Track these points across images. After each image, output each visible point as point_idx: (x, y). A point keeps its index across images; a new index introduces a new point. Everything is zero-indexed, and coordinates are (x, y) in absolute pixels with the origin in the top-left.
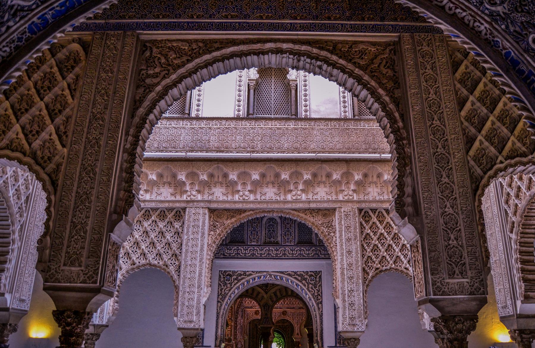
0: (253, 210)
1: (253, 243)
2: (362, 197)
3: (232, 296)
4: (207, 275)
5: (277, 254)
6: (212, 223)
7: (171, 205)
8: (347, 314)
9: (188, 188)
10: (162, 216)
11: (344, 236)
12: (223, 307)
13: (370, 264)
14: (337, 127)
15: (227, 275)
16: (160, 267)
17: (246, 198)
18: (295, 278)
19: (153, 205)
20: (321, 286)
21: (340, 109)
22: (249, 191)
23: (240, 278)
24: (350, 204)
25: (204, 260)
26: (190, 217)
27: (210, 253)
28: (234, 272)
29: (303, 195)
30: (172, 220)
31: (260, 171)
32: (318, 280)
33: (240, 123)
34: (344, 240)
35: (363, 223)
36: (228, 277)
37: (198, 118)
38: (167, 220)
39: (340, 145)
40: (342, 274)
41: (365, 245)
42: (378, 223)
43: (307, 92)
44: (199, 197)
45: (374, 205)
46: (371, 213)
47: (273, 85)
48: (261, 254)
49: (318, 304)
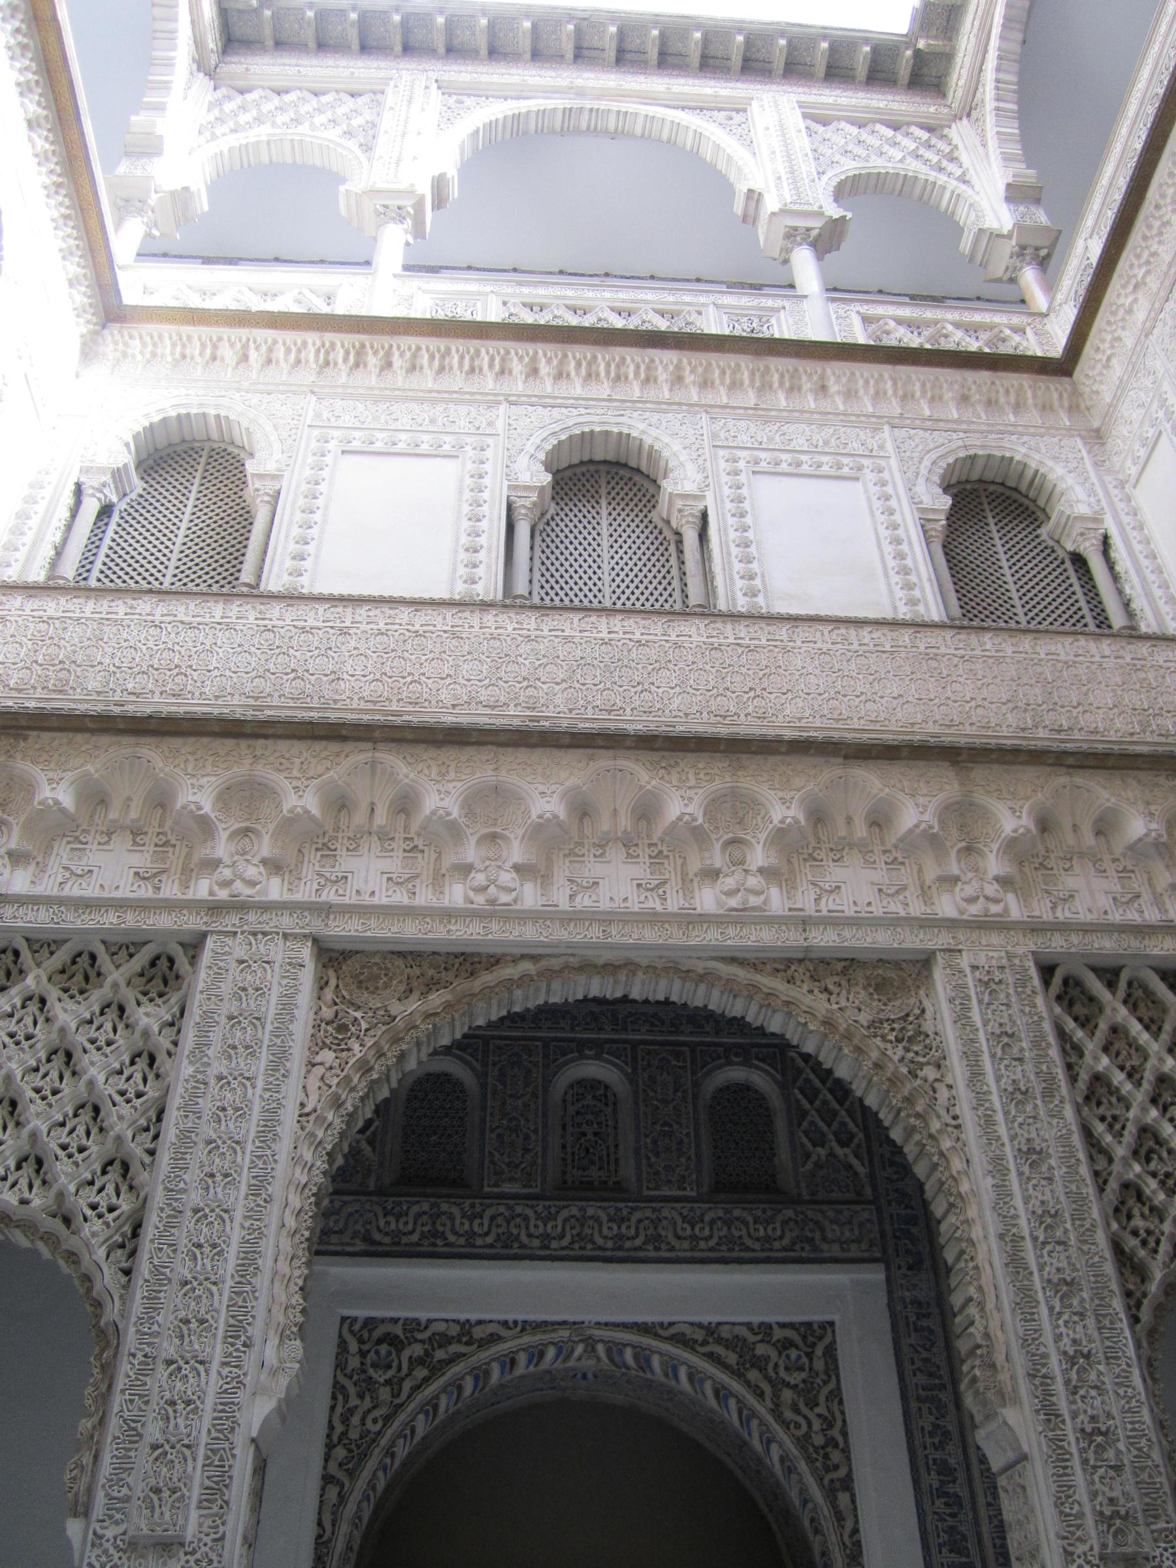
0: (533, 958)
1: (507, 1188)
2: (1042, 910)
3: (402, 1451)
4: (284, 1267)
5: (620, 1237)
6: (328, 1013)
7: (131, 920)
8: (1082, 1494)
9: (222, 848)
10: (80, 977)
11: (990, 1079)
12: (350, 1508)
13: (1138, 1222)
14: (888, 648)
15: (379, 1341)
16: (28, 1226)
17: (504, 898)
18: (711, 1357)
19: (41, 919)
20: (836, 1395)
21: (891, 592)
22: (517, 868)
23: (440, 1355)
24: (996, 939)
25: (276, 1189)
26: (219, 974)
27: (308, 1155)
28: (412, 1326)
29: (774, 893)
30: (129, 995)
31: (568, 783)
32: (819, 1365)
33: (474, 619)
34: (995, 1098)
35: (1070, 1025)
36: (384, 1349)
37: (292, 598)
38: (97, 997)
39: (910, 708)
40: (1015, 1263)
41: (1099, 1128)
42: (1135, 1028)
43: (750, 535)
44: (275, 890)
45: (1106, 946)
46: (1096, 986)
47: (605, 523)
48: (546, 1236)
49: (831, 1494)
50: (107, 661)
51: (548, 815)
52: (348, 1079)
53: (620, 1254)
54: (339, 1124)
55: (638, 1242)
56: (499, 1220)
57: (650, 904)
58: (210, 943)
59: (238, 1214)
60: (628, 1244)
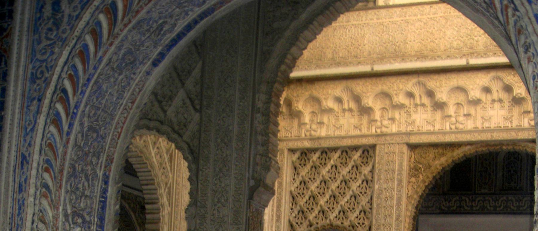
1: (483, 191)
17: (461, 126)
22: (465, 115)
27: (410, 208)
44: (394, 129)
50: (332, 45)
51: (474, 98)
52: (419, 186)
53: (519, 212)
54: (418, 199)
55: (525, 208)
56: (481, 202)
57: (507, 125)
58: (377, 148)
59: (394, 226)
60: (521, 209)
